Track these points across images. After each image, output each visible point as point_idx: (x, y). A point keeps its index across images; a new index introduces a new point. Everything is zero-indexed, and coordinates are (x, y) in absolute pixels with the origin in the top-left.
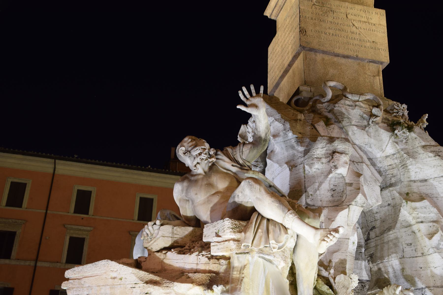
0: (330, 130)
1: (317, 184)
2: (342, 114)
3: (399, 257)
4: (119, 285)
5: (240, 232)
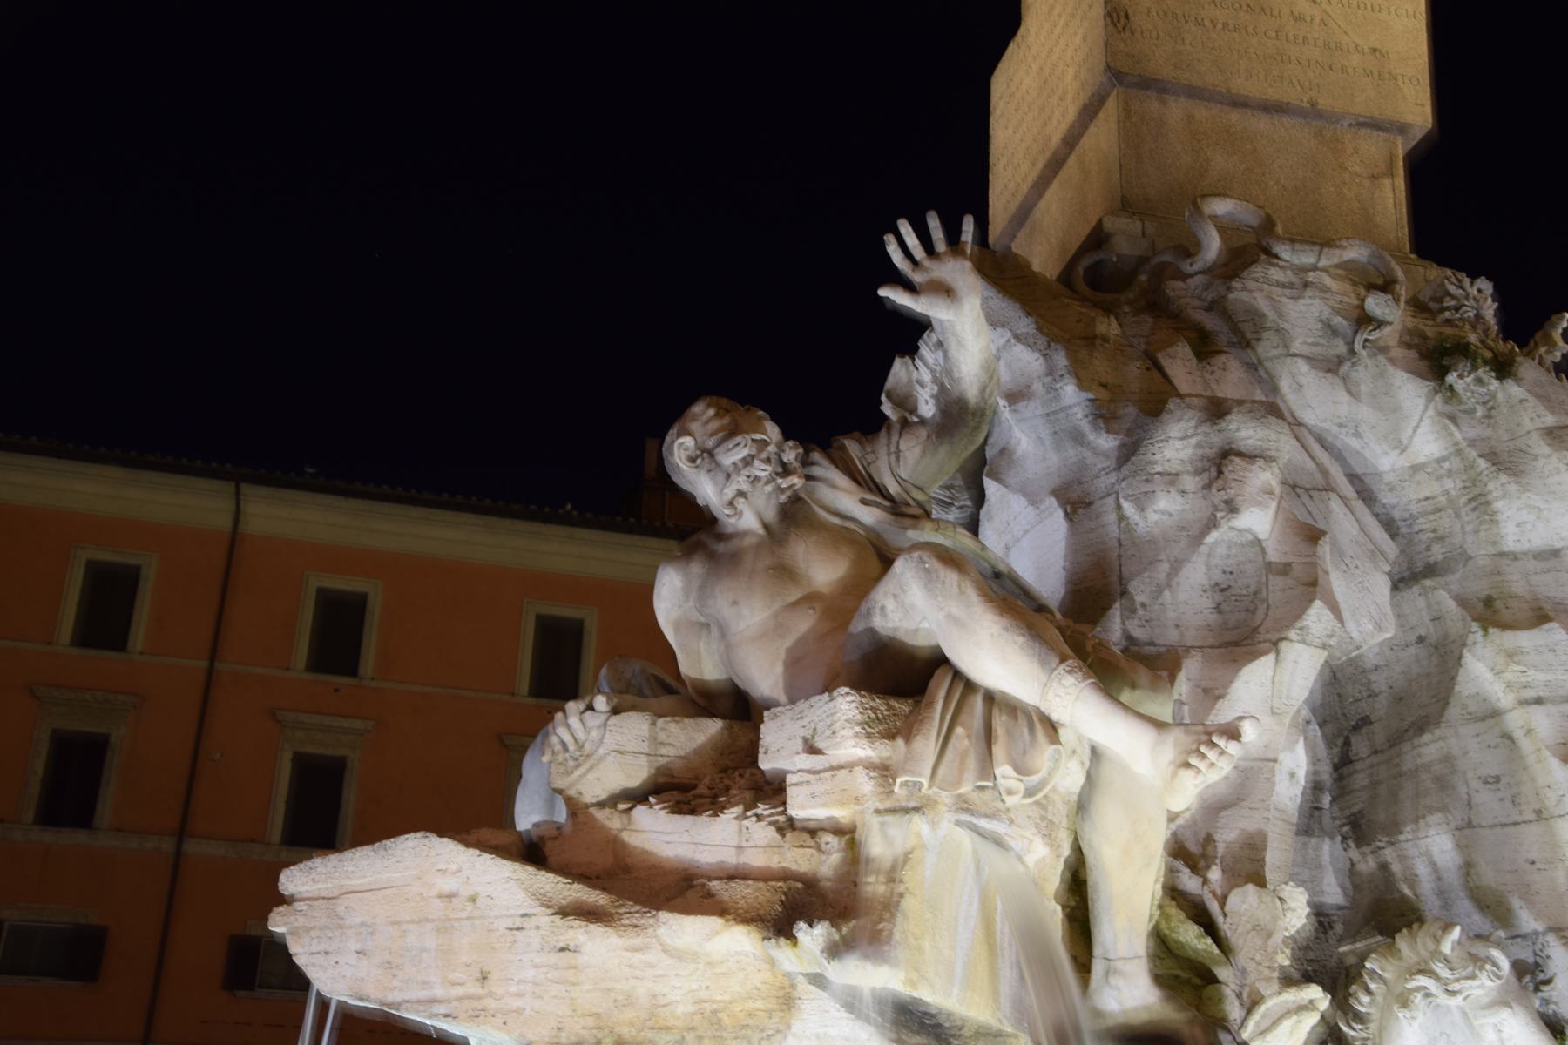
0: (1212, 372)
1: (1164, 567)
2: (1256, 317)
3: (1453, 825)
4: (469, 918)
5: (890, 736)
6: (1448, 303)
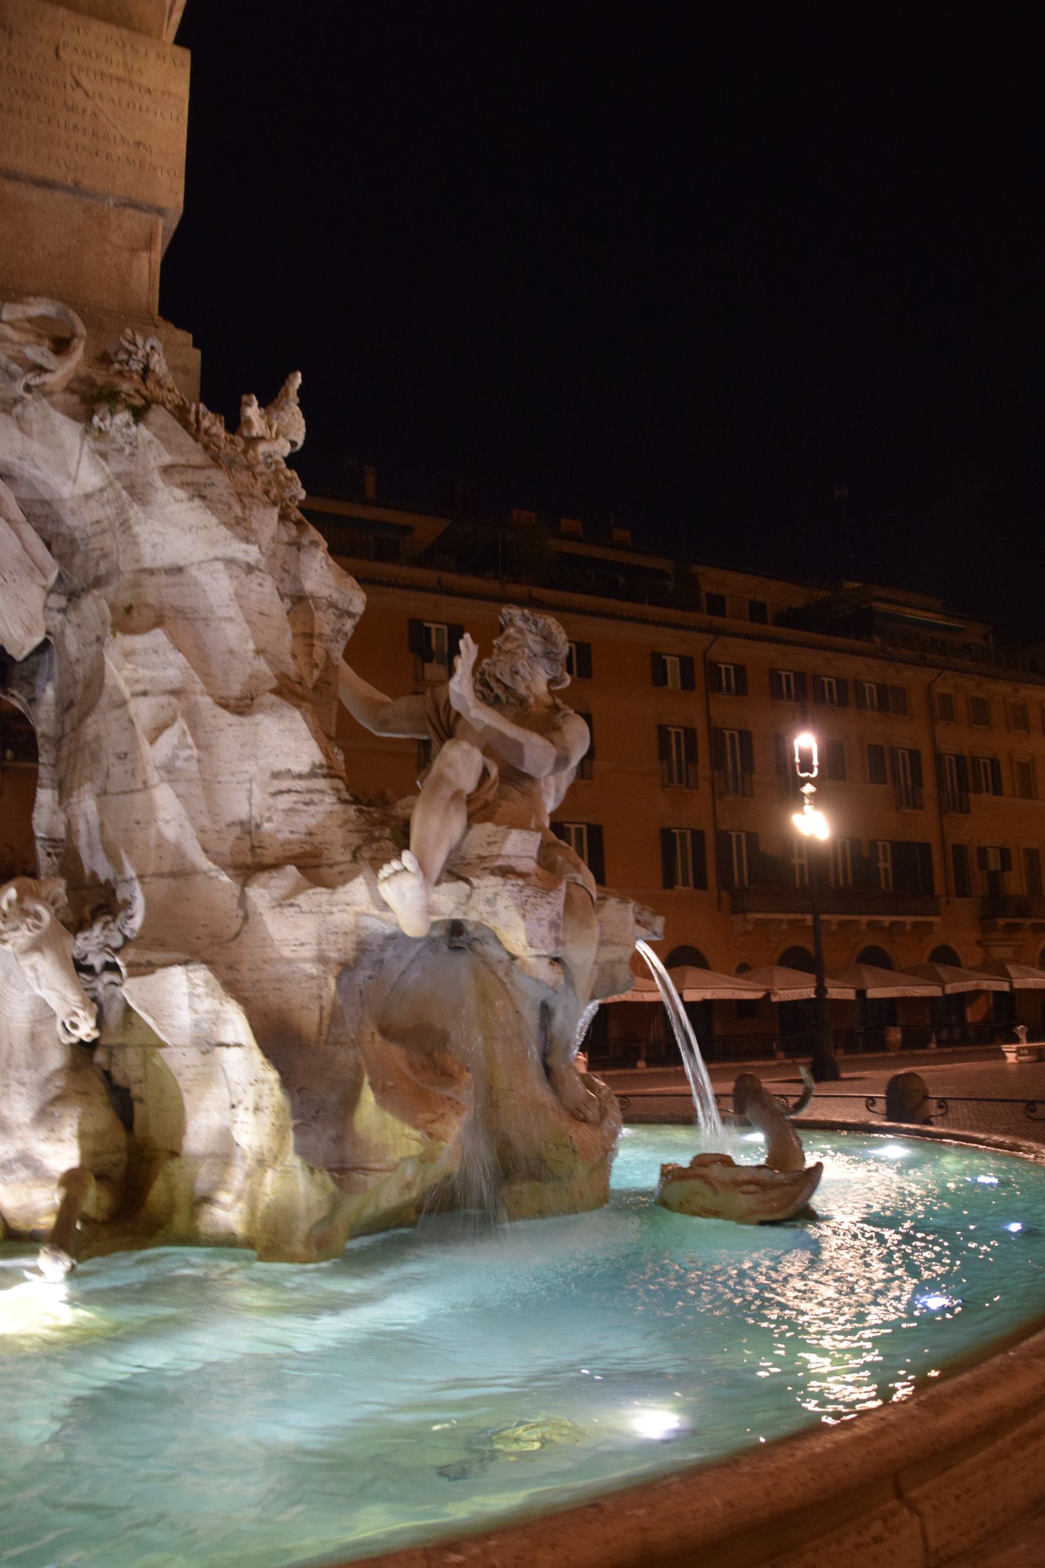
6: (123, 356)
